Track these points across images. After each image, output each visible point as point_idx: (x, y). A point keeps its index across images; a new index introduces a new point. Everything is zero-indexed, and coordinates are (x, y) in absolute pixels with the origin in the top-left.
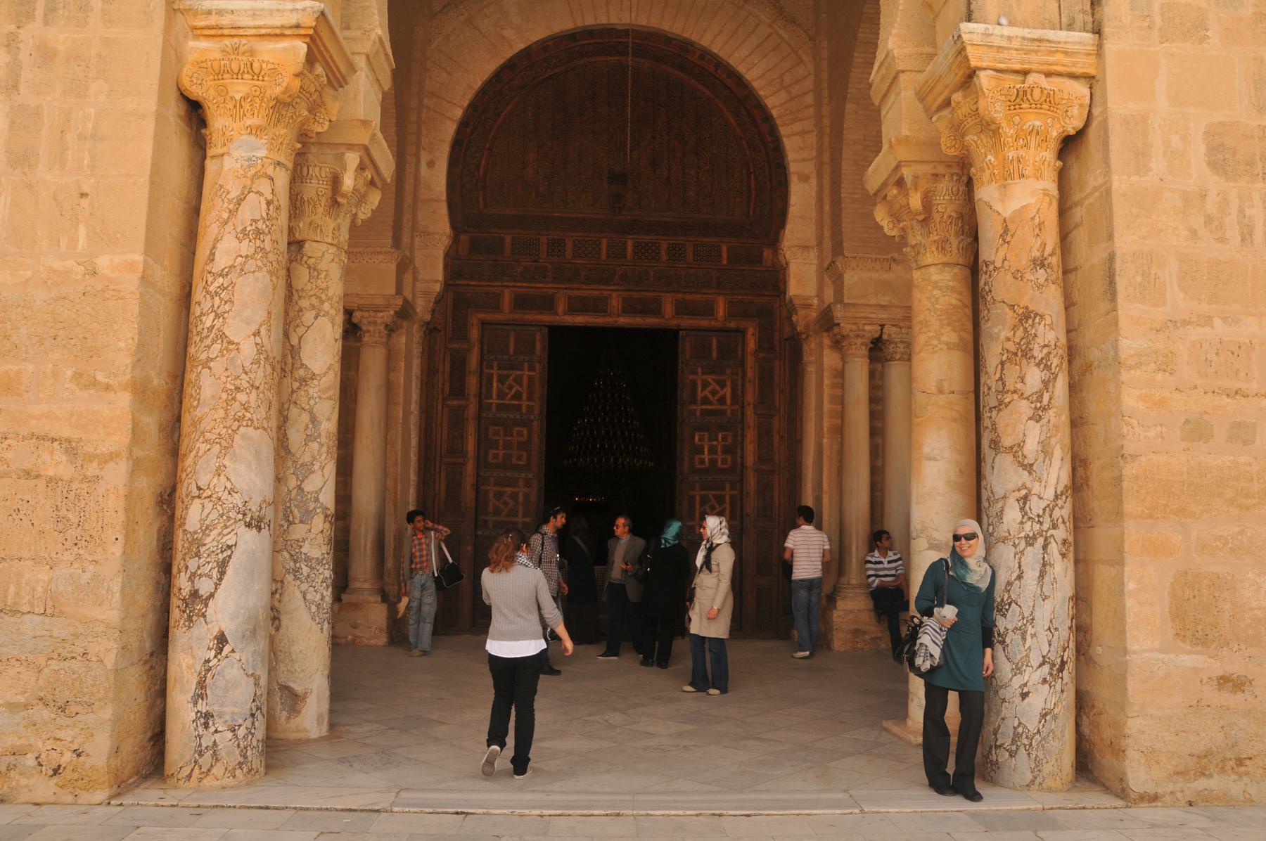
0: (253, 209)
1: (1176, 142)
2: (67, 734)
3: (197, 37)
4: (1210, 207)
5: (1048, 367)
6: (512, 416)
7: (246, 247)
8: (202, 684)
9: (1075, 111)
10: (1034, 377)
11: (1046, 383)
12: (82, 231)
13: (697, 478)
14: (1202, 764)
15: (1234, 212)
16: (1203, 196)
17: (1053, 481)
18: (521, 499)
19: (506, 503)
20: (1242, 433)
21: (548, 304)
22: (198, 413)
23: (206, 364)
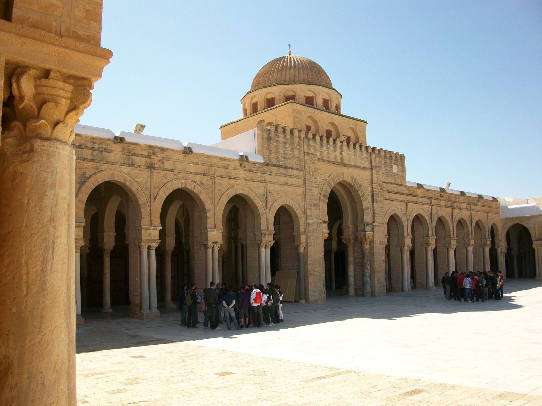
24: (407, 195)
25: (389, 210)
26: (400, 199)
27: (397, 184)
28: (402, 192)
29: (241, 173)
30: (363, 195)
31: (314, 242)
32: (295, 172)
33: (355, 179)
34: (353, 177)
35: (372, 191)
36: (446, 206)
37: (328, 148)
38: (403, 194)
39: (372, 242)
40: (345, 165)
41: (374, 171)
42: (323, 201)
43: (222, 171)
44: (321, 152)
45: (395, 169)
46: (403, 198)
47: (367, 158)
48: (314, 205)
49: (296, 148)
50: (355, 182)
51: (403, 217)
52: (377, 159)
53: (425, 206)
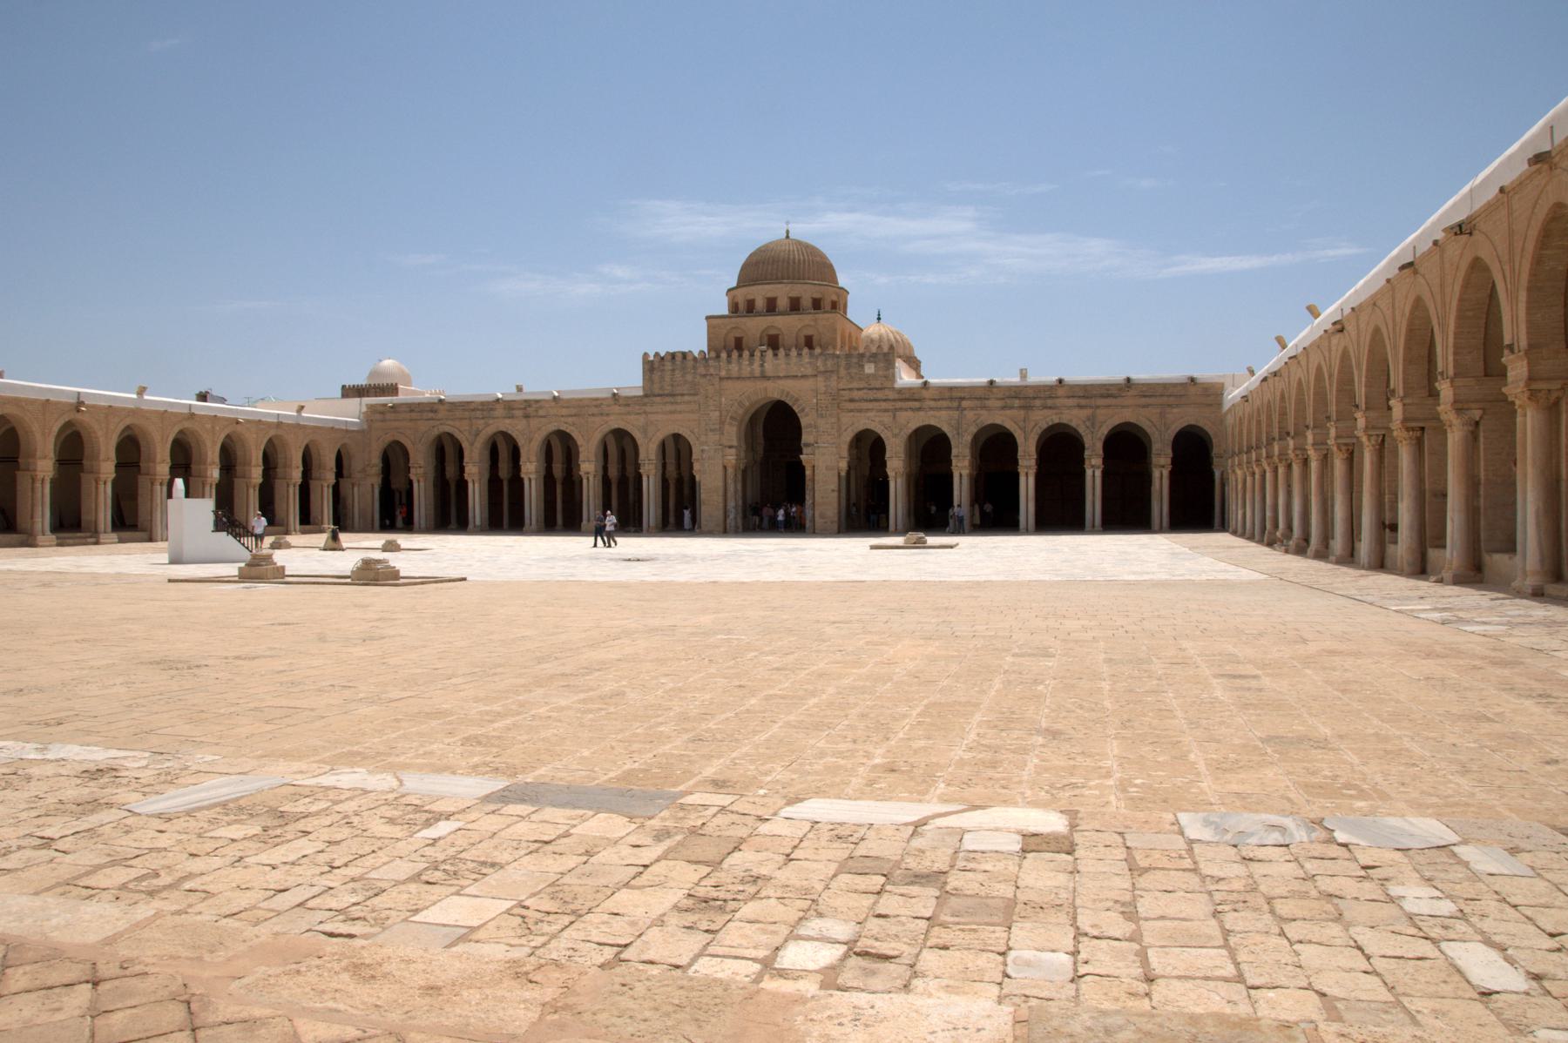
29: (617, 409)
32: (686, 398)
36: (1003, 408)
37: (740, 364)
40: (768, 378)
41: (820, 379)
43: (595, 411)
45: (869, 369)
46: (884, 405)
52: (830, 363)
53: (944, 413)
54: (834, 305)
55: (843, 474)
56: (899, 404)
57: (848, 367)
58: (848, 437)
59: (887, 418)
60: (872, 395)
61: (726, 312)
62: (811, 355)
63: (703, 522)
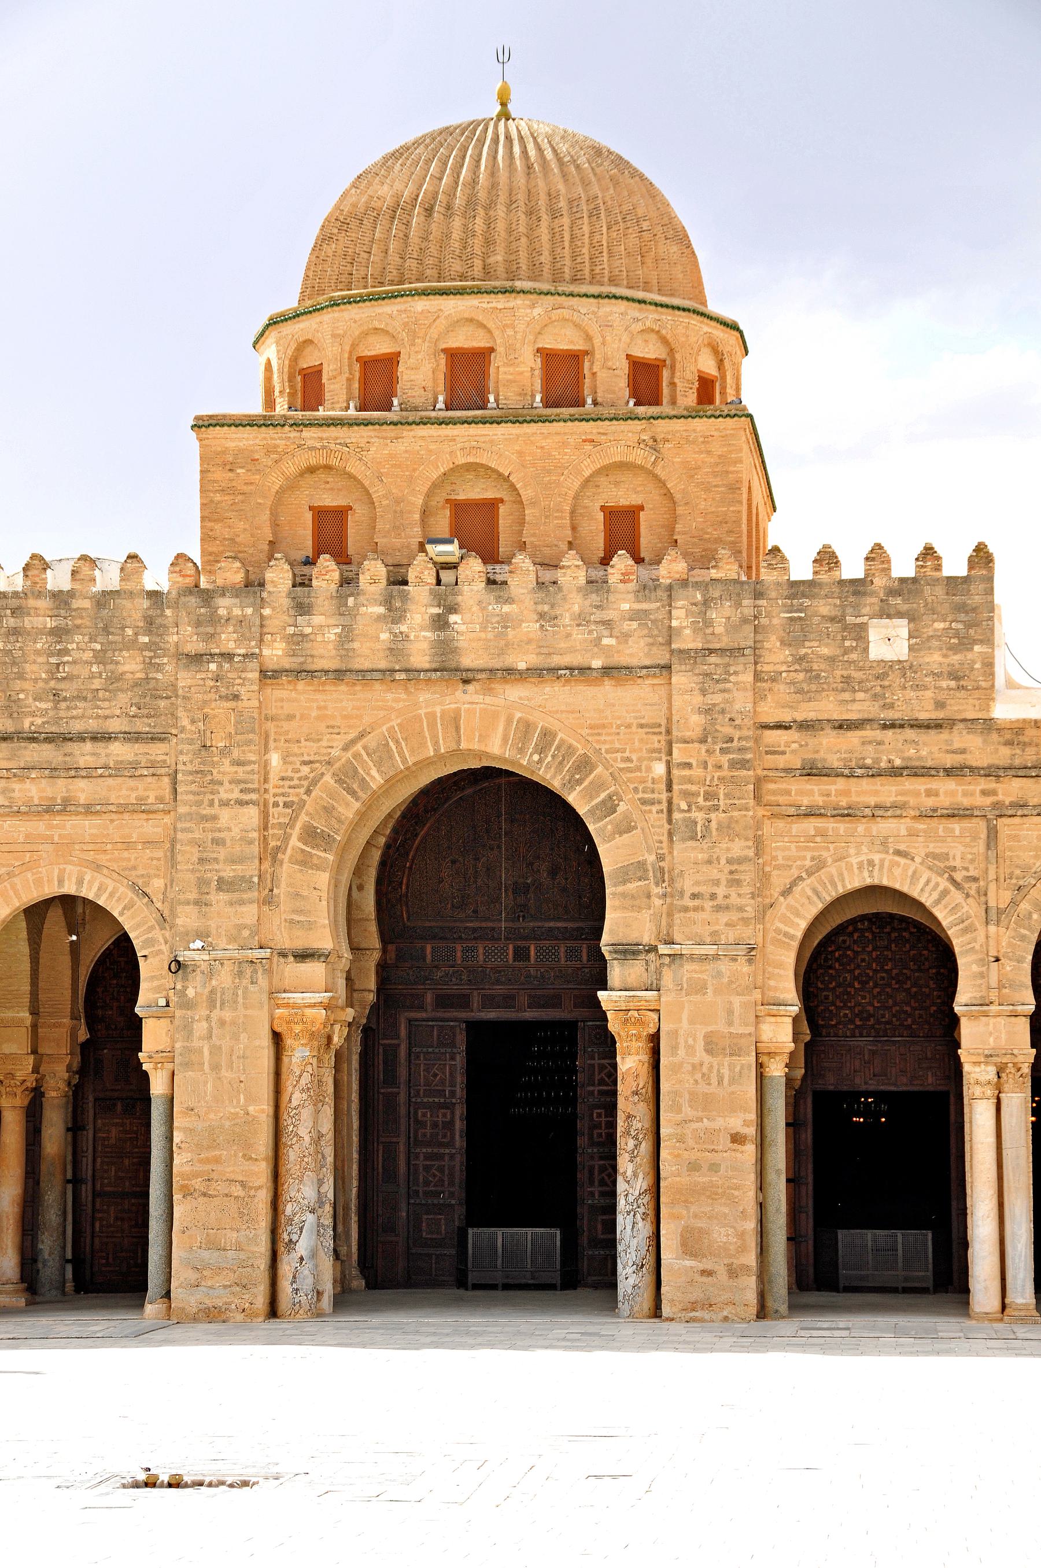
0: (306, 1079)
1: (690, 1041)
2: (246, 1297)
3: (278, 1008)
4: (705, 1070)
5: (637, 1139)
6: (436, 1100)
7: (305, 1096)
8: (294, 1277)
9: (651, 1025)
10: (631, 1143)
11: (636, 1146)
12: (242, 1096)
13: (595, 1150)
14: (693, 1306)
15: (715, 1071)
16: (701, 1065)
17: (638, 1188)
18: (447, 1172)
19: (435, 1176)
20: (714, 1167)
21: (464, 1002)
22: (289, 1167)
23: (291, 1146)
24: (992, 772)
25: (820, 865)
26: (930, 802)
27: (893, 726)
28: (949, 761)
30: (609, 807)
31: (215, 1050)
32: (119, 751)
33: (547, 735)
34: (527, 727)
35: (669, 788)
38: (949, 772)
39: (655, 1039)
41: (679, 679)
42: (304, 861)
44: (298, 640)
45: (888, 641)
46: (950, 792)
47: (635, 616)
48: (223, 885)
49: (132, 644)
50: (541, 750)
51: (957, 896)
52: (720, 616)
54: (706, 389)
55: (777, 1070)
56: (1011, 789)
57: (798, 632)
58: (796, 918)
59: (961, 844)
60: (896, 747)
61: (255, 407)
62: (647, 589)
63: (180, 1274)
